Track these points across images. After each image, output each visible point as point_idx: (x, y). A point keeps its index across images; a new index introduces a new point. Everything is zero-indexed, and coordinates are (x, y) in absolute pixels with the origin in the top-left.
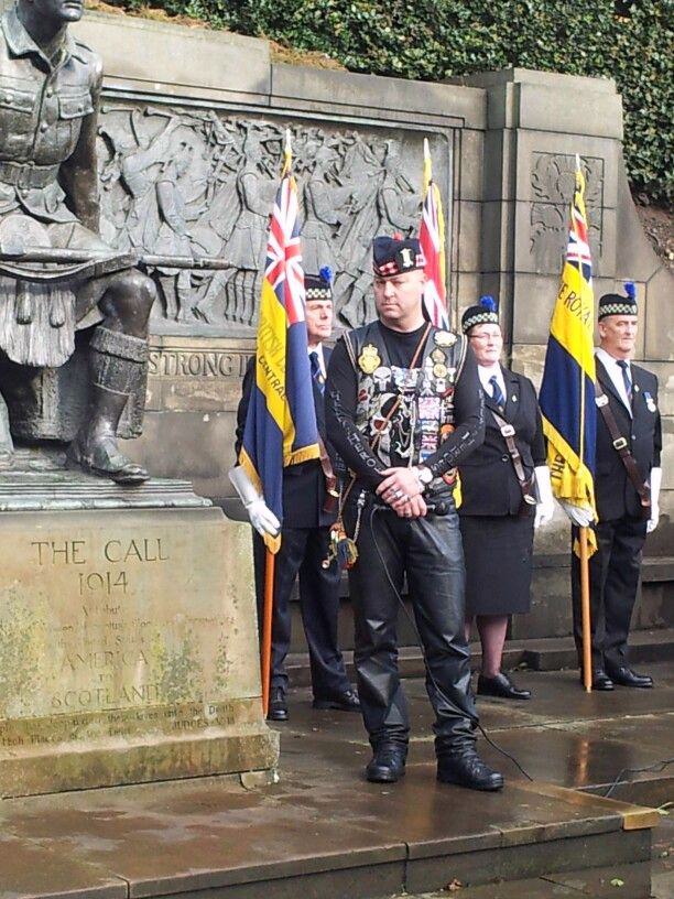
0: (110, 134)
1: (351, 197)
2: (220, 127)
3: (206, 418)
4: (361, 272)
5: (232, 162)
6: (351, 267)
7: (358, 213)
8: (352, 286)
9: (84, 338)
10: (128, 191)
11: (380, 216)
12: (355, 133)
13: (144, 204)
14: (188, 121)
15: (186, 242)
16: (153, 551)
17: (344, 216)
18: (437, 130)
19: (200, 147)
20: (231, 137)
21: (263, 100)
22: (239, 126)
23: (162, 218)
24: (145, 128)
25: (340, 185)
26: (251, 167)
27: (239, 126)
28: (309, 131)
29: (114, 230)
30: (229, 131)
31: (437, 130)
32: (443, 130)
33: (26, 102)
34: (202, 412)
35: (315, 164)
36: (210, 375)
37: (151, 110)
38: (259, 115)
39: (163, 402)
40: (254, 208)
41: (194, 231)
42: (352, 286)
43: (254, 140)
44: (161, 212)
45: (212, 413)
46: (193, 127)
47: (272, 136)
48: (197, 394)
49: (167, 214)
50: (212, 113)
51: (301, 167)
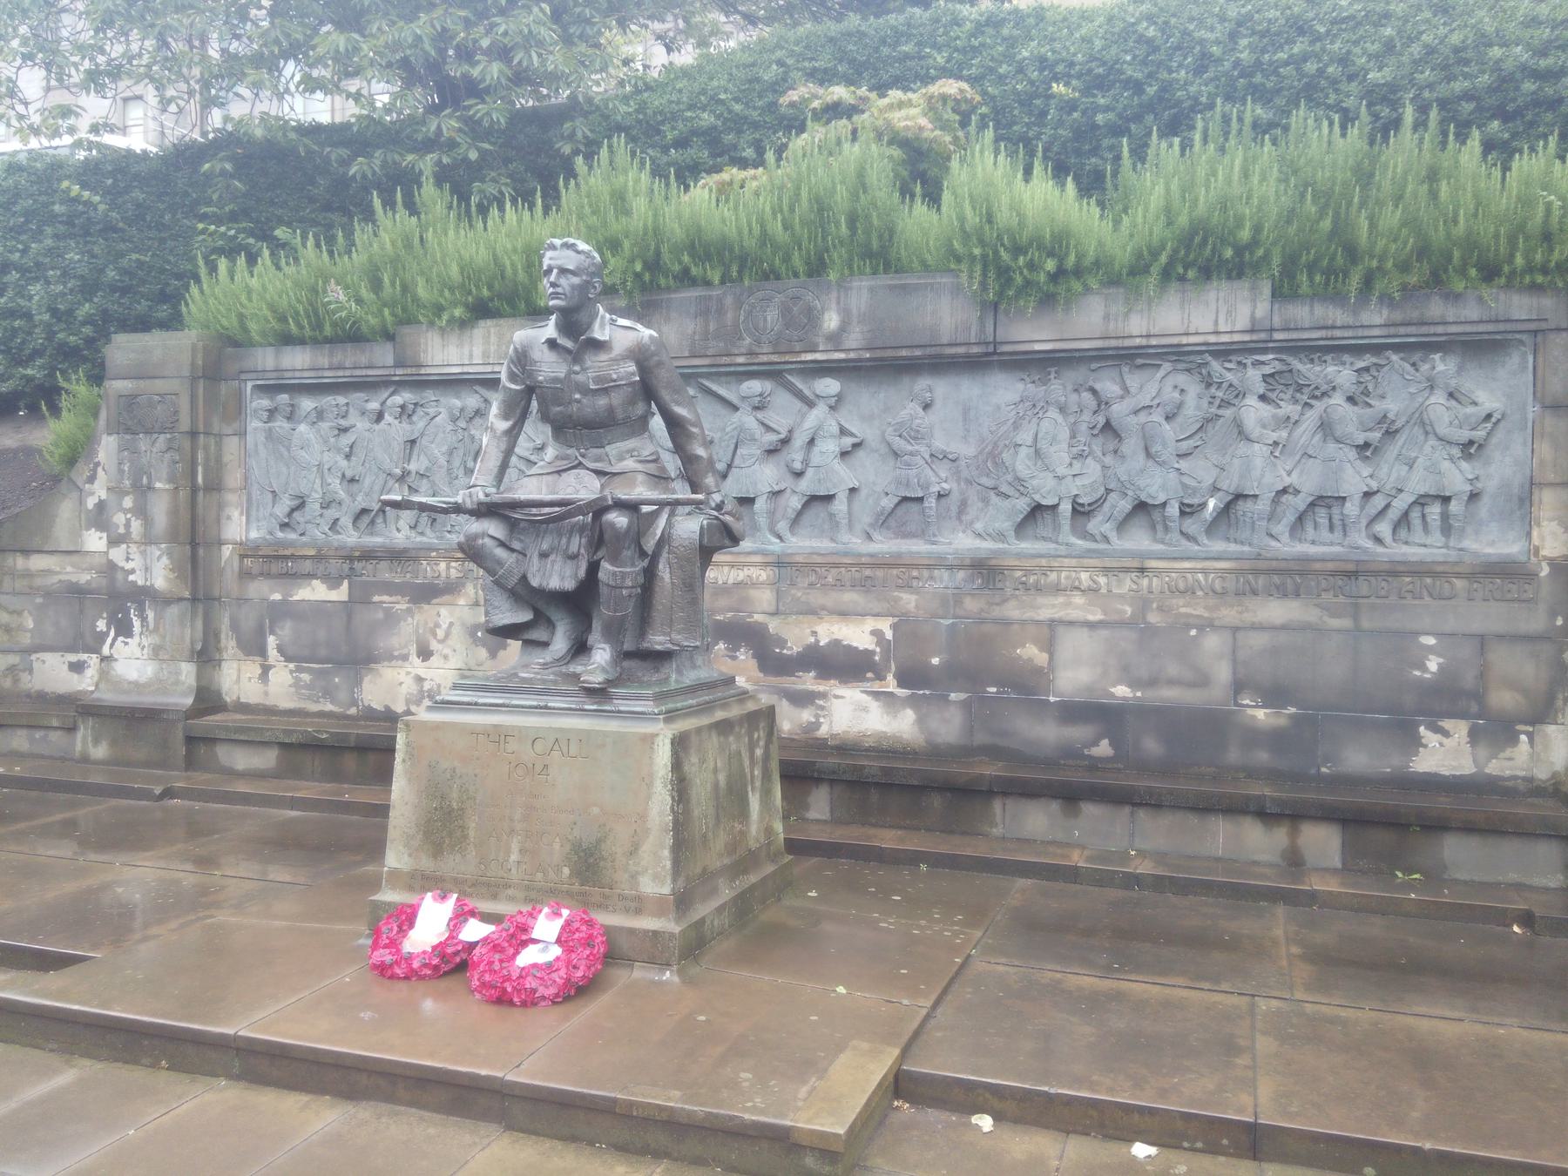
0: (1098, 386)
1: (1385, 416)
2: (1215, 365)
3: (1193, 632)
4: (1401, 491)
5: (1229, 397)
6: (1388, 487)
7: (1397, 431)
8: (1388, 506)
9: (593, 568)
10: (1117, 435)
11: (1427, 433)
12: (1389, 353)
13: (1131, 445)
14: (1181, 366)
15: (1173, 475)
16: (574, 750)
17: (1375, 436)
18: (1509, 336)
19: (1194, 388)
20: (1229, 376)
21: (1263, 336)
22: (1239, 363)
23: (1148, 455)
24: (1133, 380)
25: (1370, 406)
26: (1252, 401)
27: (1239, 363)
28: (1328, 358)
29: (1099, 467)
30: (1229, 370)
31: (1509, 336)
32: (1518, 336)
33: (556, 380)
34: (1189, 626)
35: (1334, 388)
36: (1200, 593)
37: (1140, 361)
38: (1265, 351)
39: (1144, 618)
40: (1252, 437)
41: (1183, 465)
42: (1388, 506)
43: (1254, 376)
44: (1146, 449)
45: (1201, 629)
46: (1188, 370)
47: (1278, 366)
48: (1183, 610)
49: (1153, 450)
50: (1209, 358)
51: (1317, 393)
